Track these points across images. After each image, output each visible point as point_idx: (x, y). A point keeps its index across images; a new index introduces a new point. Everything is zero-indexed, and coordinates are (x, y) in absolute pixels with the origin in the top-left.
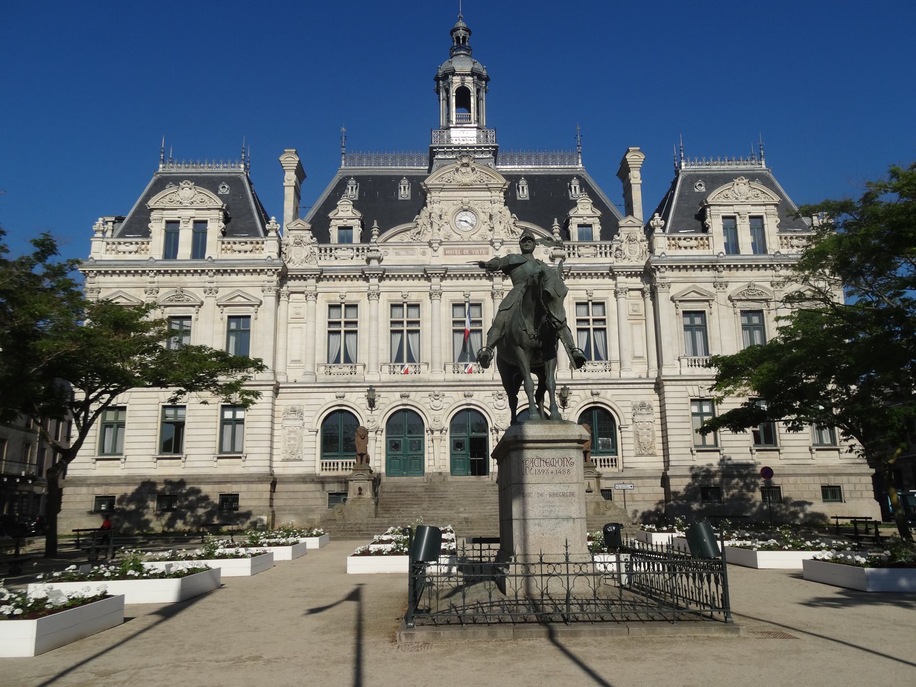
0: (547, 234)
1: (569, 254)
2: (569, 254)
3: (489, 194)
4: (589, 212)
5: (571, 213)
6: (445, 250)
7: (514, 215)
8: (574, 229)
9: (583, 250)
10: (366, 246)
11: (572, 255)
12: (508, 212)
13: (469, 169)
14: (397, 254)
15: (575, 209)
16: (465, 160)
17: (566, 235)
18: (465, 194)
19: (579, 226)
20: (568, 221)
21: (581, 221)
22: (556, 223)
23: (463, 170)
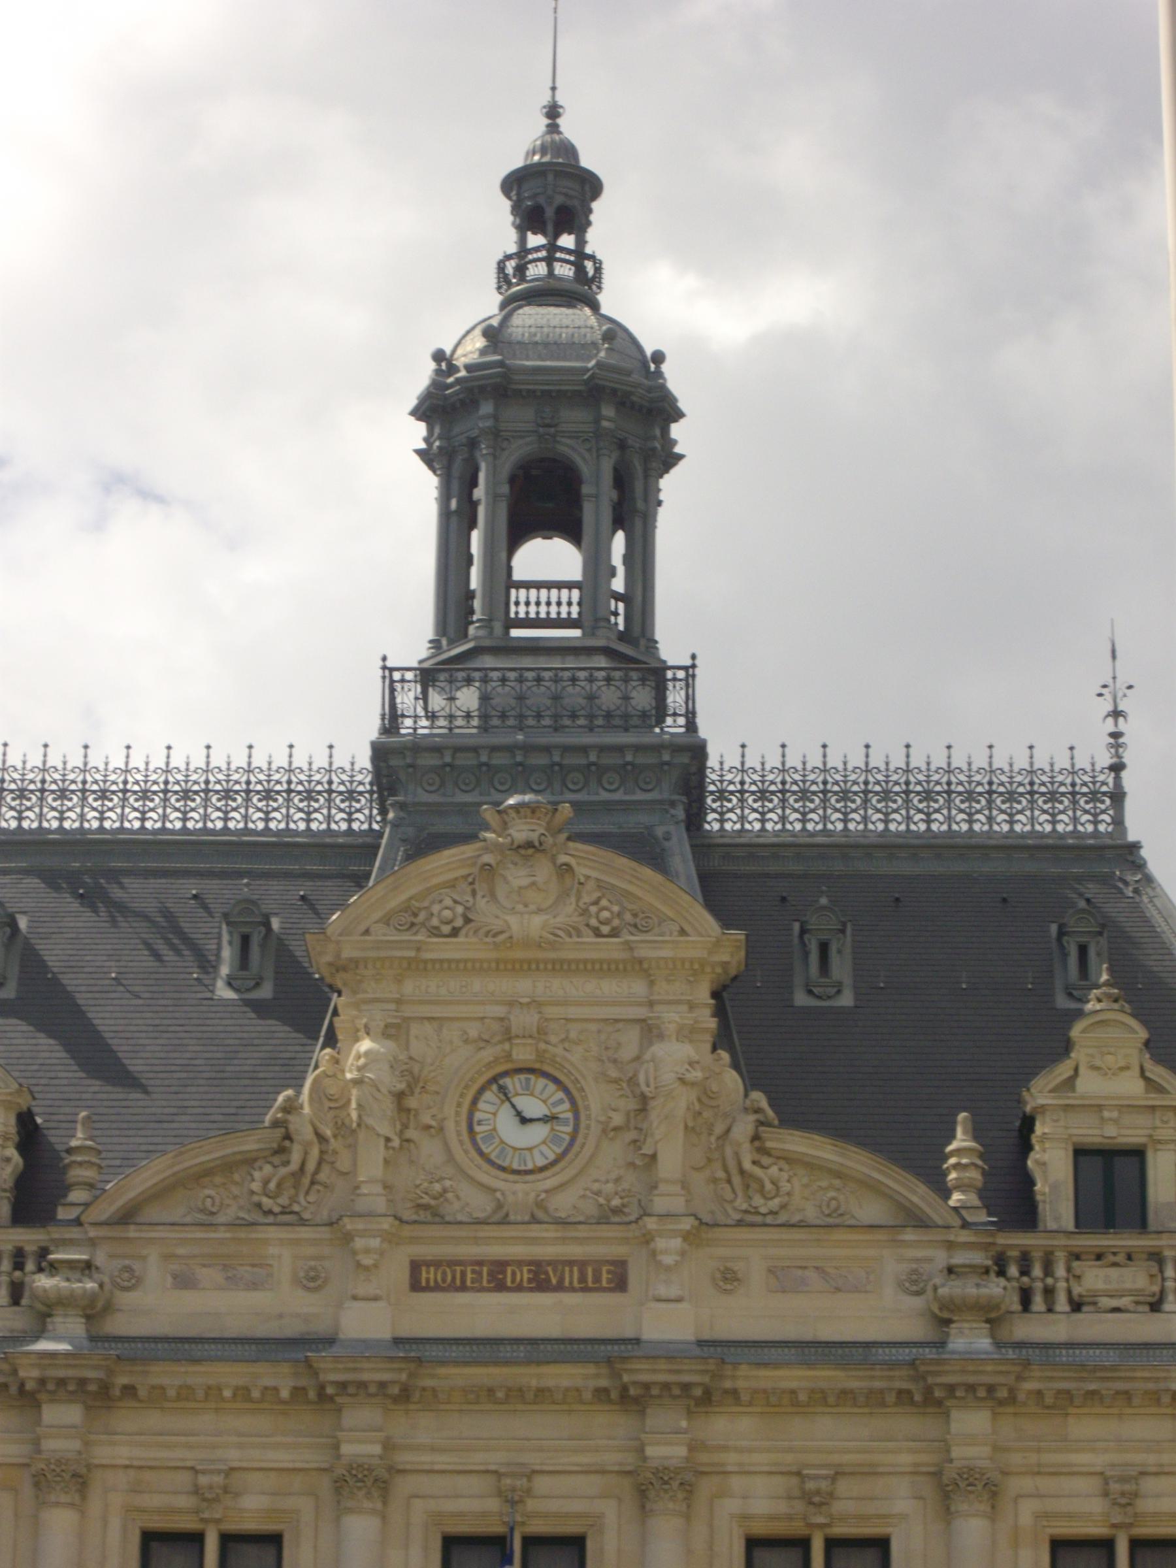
0: (918, 1194)
1: (1026, 1299)
2: (1026, 1299)
3: (638, 988)
4: (1131, 1086)
5: (1039, 1094)
6: (415, 1266)
7: (759, 1098)
8: (1052, 1167)
9: (1094, 1278)
10: (29, 1238)
11: (1038, 1303)
12: (732, 1080)
13: (543, 871)
14: (184, 1282)
15: (1063, 1070)
16: (521, 831)
17: (1013, 1199)
18: (523, 986)
19: (1080, 1153)
20: (1028, 1123)
21: (1093, 1133)
22: (961, 1140)
23: (517, 876)
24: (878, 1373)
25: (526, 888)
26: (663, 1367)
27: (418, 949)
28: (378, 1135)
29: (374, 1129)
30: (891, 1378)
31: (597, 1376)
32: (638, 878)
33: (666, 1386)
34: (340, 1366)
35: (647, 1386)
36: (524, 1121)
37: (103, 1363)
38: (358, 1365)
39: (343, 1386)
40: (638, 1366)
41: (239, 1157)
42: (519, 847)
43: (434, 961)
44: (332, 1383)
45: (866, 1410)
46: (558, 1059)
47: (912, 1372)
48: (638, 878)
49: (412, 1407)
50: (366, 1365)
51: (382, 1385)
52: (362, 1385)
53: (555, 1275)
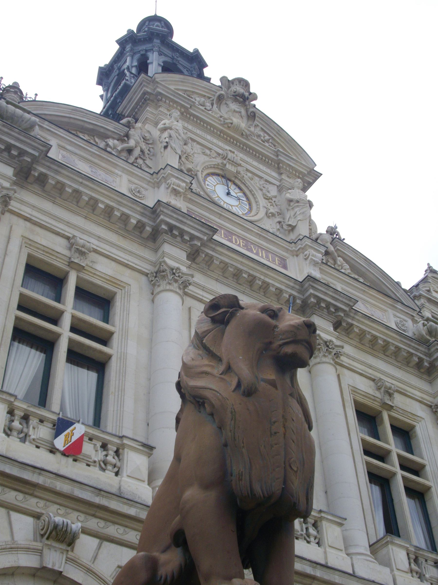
24: (413, 344)
25: (237, 112)
26: (331, 293)
27: (191, 107)
28: (176, 153)
29: (175, 149)
30: (417, 350)
31: (293, 288)
32: (280, 135)
33: (329, 305)
34: (175, 216)
35: (319, 300)
36: (228, 194)
37: (41, 148)
38: (185, 220)
39: (171, 228)
40: (320, 288)
41: (102, 130)
42: (236, 96)
43: (195, 116)
44: (167, 224)
45: (399, 365)
46: (244, 178)
47: (427, 351)
48: (280, 135)
49: (194, 265)
50: (188, 222)
51: (193, 237)
52: (182, 233)
53: (255, 250)
